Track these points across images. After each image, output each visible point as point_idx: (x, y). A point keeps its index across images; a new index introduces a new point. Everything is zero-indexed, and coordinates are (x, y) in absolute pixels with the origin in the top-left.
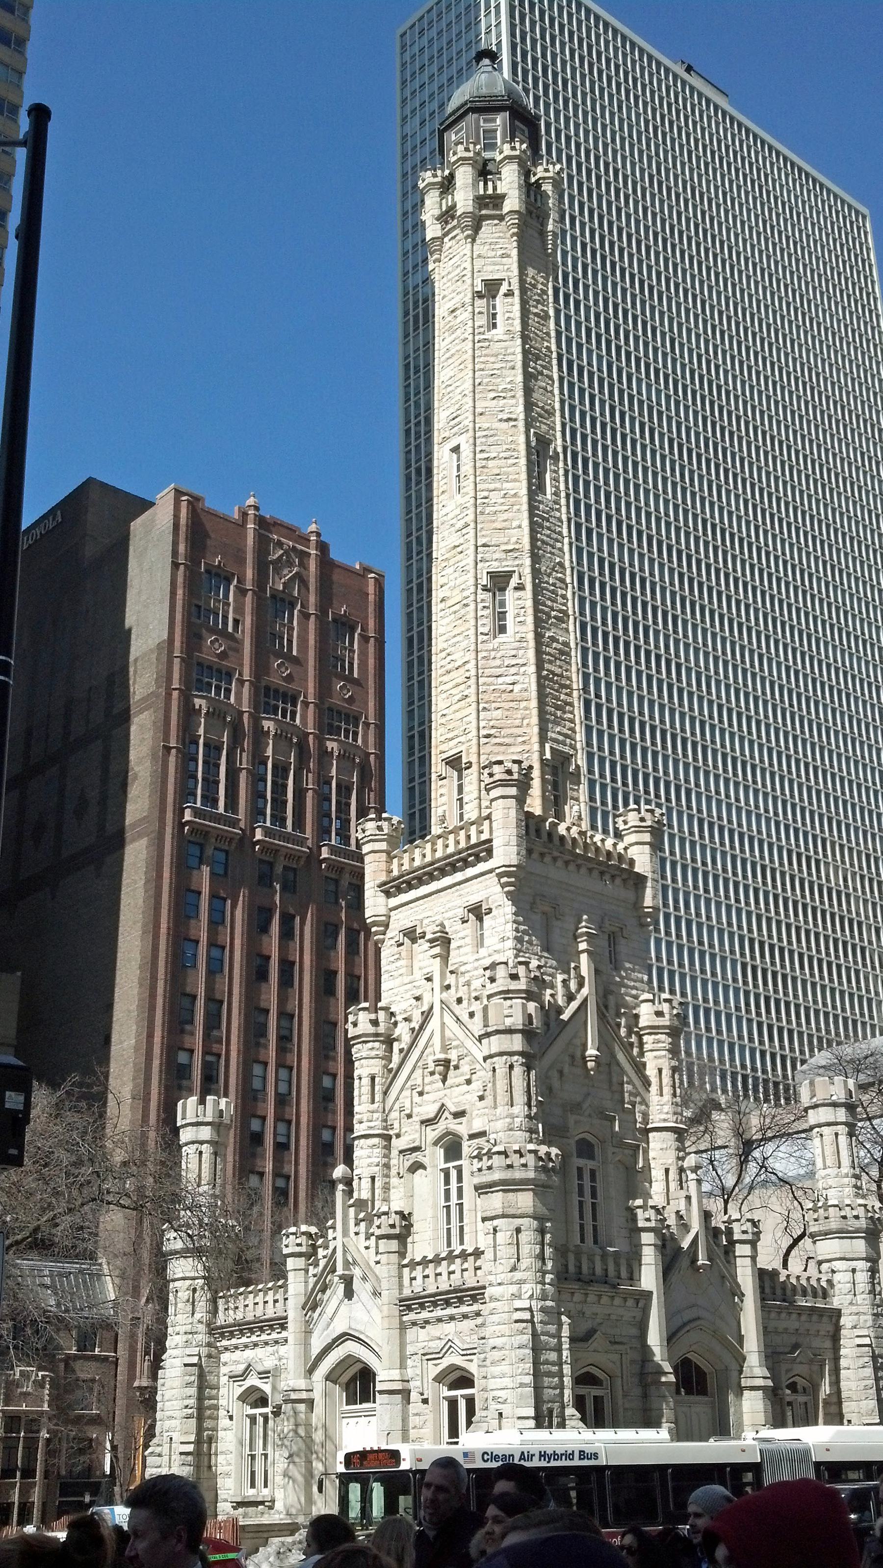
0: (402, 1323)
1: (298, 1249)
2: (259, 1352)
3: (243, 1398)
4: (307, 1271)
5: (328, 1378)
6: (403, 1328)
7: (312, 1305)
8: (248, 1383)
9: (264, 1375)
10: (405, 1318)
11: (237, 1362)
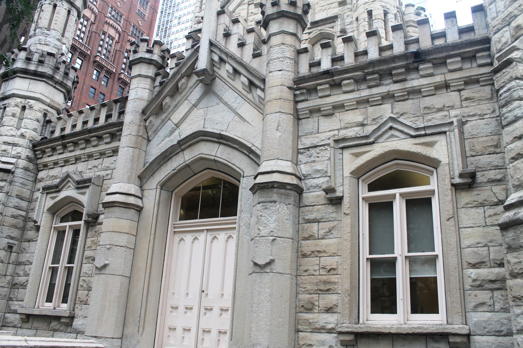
0: (296, 110)
1: (147, 56)
2: (81, 166)
3: (53, 211)
4: (154, 80)
5: (163, 186)
6: (298, 118)
7: (155, 109)
8: (62, 195)
9: (83, 184)
10: (300, 106)
11: (56, 177)
